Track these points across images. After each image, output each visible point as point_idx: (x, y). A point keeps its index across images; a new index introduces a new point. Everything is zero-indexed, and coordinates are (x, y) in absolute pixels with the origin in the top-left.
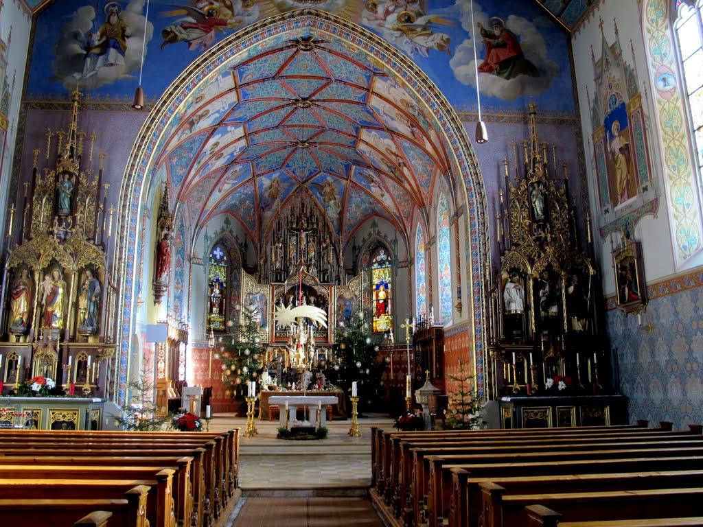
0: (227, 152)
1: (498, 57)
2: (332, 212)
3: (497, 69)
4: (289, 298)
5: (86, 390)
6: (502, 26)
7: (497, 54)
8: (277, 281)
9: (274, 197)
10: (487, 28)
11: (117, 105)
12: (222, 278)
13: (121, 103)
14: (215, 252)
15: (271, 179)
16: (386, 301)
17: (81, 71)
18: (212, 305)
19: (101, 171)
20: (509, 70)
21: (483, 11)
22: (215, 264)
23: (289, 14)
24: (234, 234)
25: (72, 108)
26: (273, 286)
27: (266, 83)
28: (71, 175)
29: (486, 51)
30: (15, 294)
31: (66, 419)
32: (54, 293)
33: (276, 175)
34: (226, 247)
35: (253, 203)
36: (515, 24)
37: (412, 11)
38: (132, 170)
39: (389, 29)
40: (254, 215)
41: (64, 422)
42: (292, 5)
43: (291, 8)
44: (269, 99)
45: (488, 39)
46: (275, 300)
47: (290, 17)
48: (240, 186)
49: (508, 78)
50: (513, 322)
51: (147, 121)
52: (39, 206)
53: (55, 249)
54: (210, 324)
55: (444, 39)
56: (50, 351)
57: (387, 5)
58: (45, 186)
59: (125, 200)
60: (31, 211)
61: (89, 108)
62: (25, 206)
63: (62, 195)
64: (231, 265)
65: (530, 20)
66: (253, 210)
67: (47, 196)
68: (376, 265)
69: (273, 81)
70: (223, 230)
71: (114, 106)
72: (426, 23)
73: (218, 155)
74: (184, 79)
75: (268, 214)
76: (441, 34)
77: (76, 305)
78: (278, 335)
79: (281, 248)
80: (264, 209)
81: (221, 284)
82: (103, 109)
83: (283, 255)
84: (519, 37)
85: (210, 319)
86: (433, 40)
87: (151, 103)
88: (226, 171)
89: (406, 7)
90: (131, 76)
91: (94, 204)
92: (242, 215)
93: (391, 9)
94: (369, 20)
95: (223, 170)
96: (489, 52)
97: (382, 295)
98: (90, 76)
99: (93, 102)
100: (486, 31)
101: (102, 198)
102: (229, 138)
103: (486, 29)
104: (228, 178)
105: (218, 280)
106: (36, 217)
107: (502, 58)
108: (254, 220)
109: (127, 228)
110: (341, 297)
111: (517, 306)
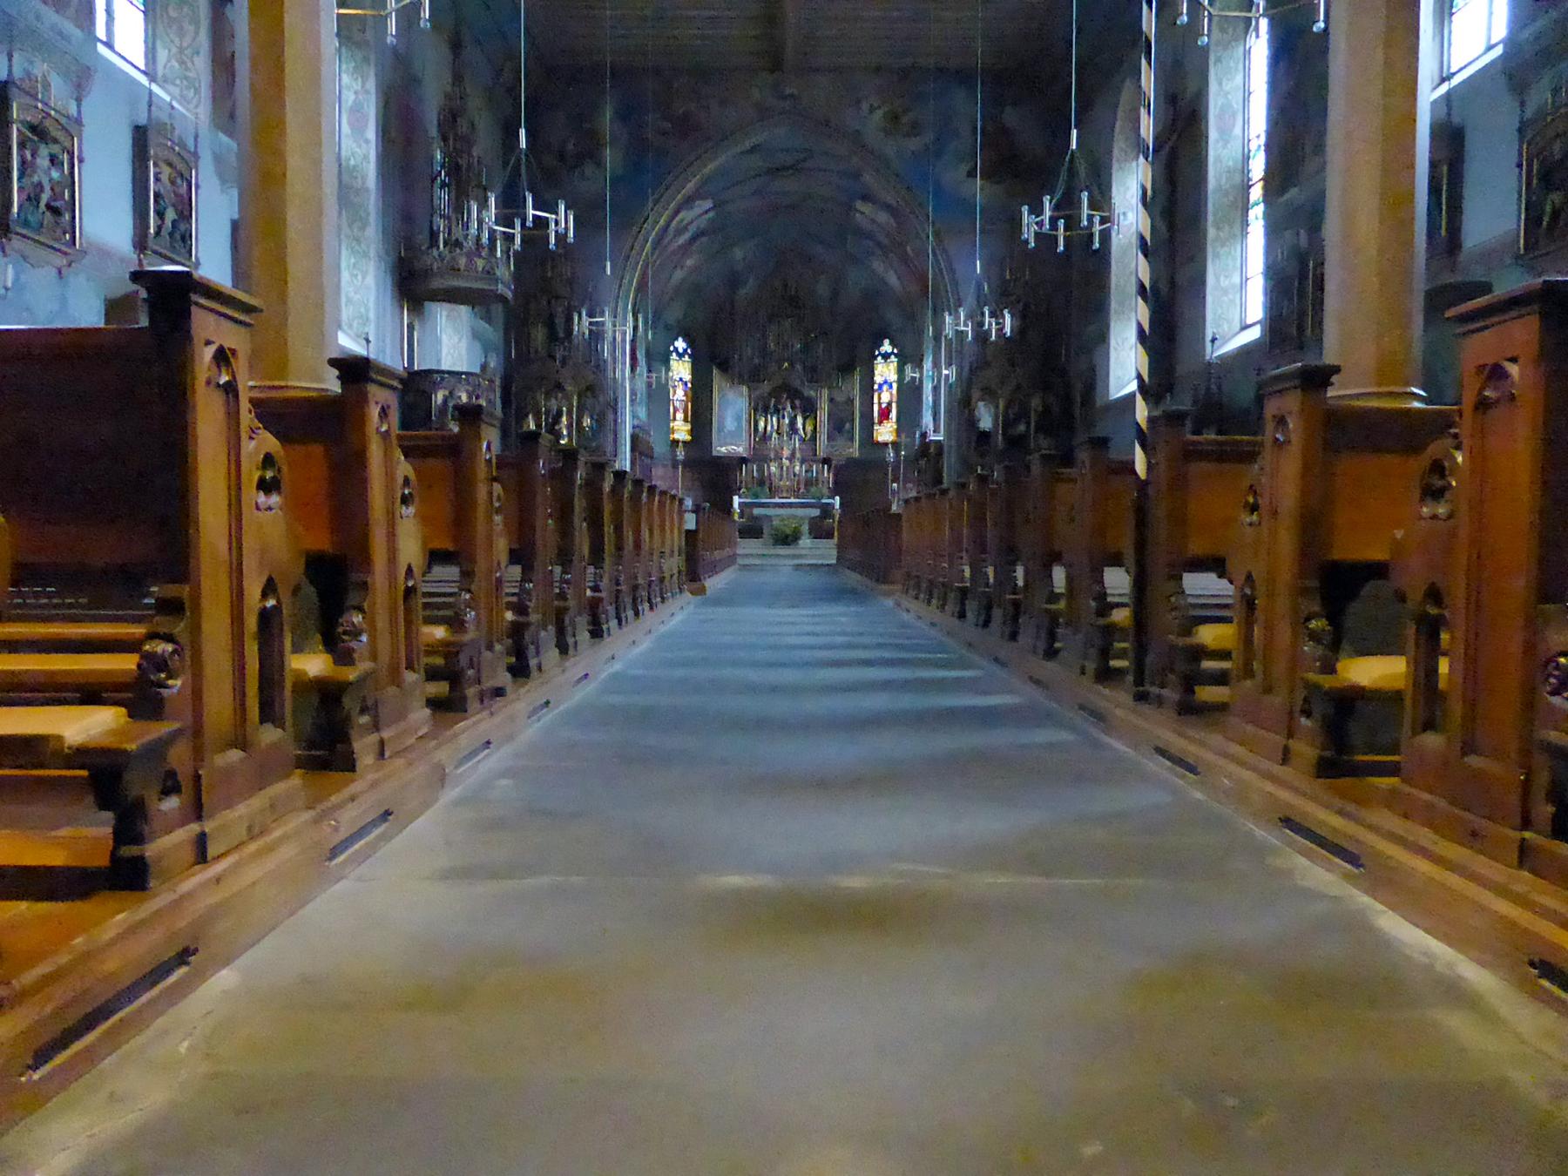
2: (823, 289)
14: (676, 344)
16: (889, 404)
18: (676, 410)
32: (559, 414)
36: (1011, 116)
50: (984, 436)
51: (630, 240)
68: (879, 358)
73: (679, 232)
75: (742, 292)
77: (579, 422)
81: (686, 384)
93: (876, 105)
97: (885, 397)
102: (697, 211)
105: (681, 379)
110: (831, 400)
111: (986, 422)
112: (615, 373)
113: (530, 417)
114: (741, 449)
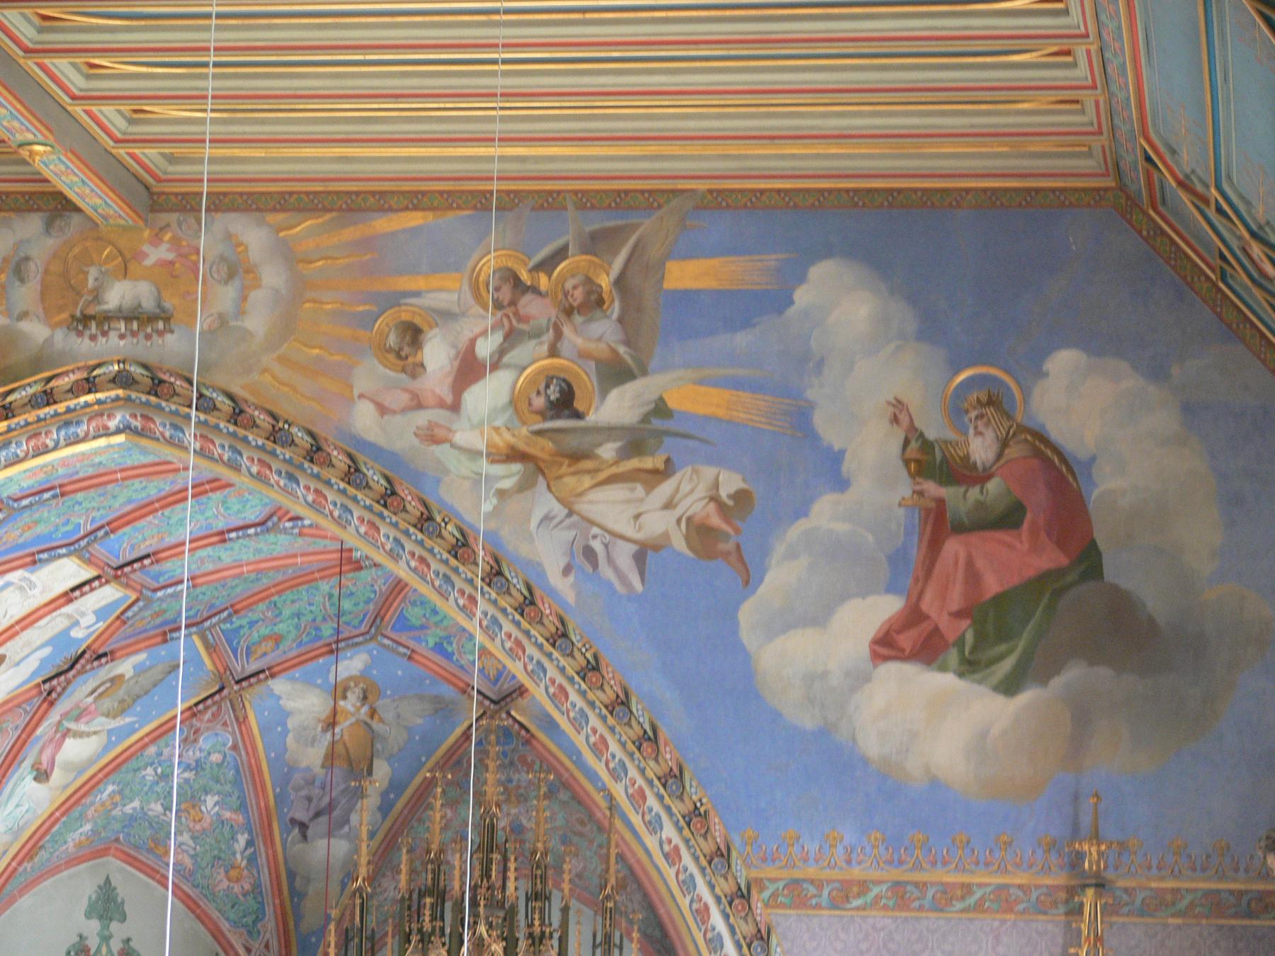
1: (973, 577)
3: (960, 642)
6: (1009, 417)
7: (970, 564)
10: (935, 428)
20: (1022, 644)
21: (921, 336)
23: (37, 388)
29: (915, 553)
33: (353, 664)
35: (242, 807)
37: (583, 355)
39: (474, 454)
40: (252, 860)
42: (49, 342)
43: (37, 363)
45: (931, 488)
47: (33, 403)
49: (1009, 687)
55: (724, 493)
57: (467, 329)
65: (1157, 372)
66: (242, 839)
72: (645, 419)
76: (709, 472)
80: (303, 827)
84: (1093, 459)
86: (669, 505)
89: (559, 335)
93: (485, 349)
94: (383, 410)
96: (935, 545)
100: (927, 446)
103: (931, 435)
104: (80, 714)
107: (992, 585)
108: (257, 888)
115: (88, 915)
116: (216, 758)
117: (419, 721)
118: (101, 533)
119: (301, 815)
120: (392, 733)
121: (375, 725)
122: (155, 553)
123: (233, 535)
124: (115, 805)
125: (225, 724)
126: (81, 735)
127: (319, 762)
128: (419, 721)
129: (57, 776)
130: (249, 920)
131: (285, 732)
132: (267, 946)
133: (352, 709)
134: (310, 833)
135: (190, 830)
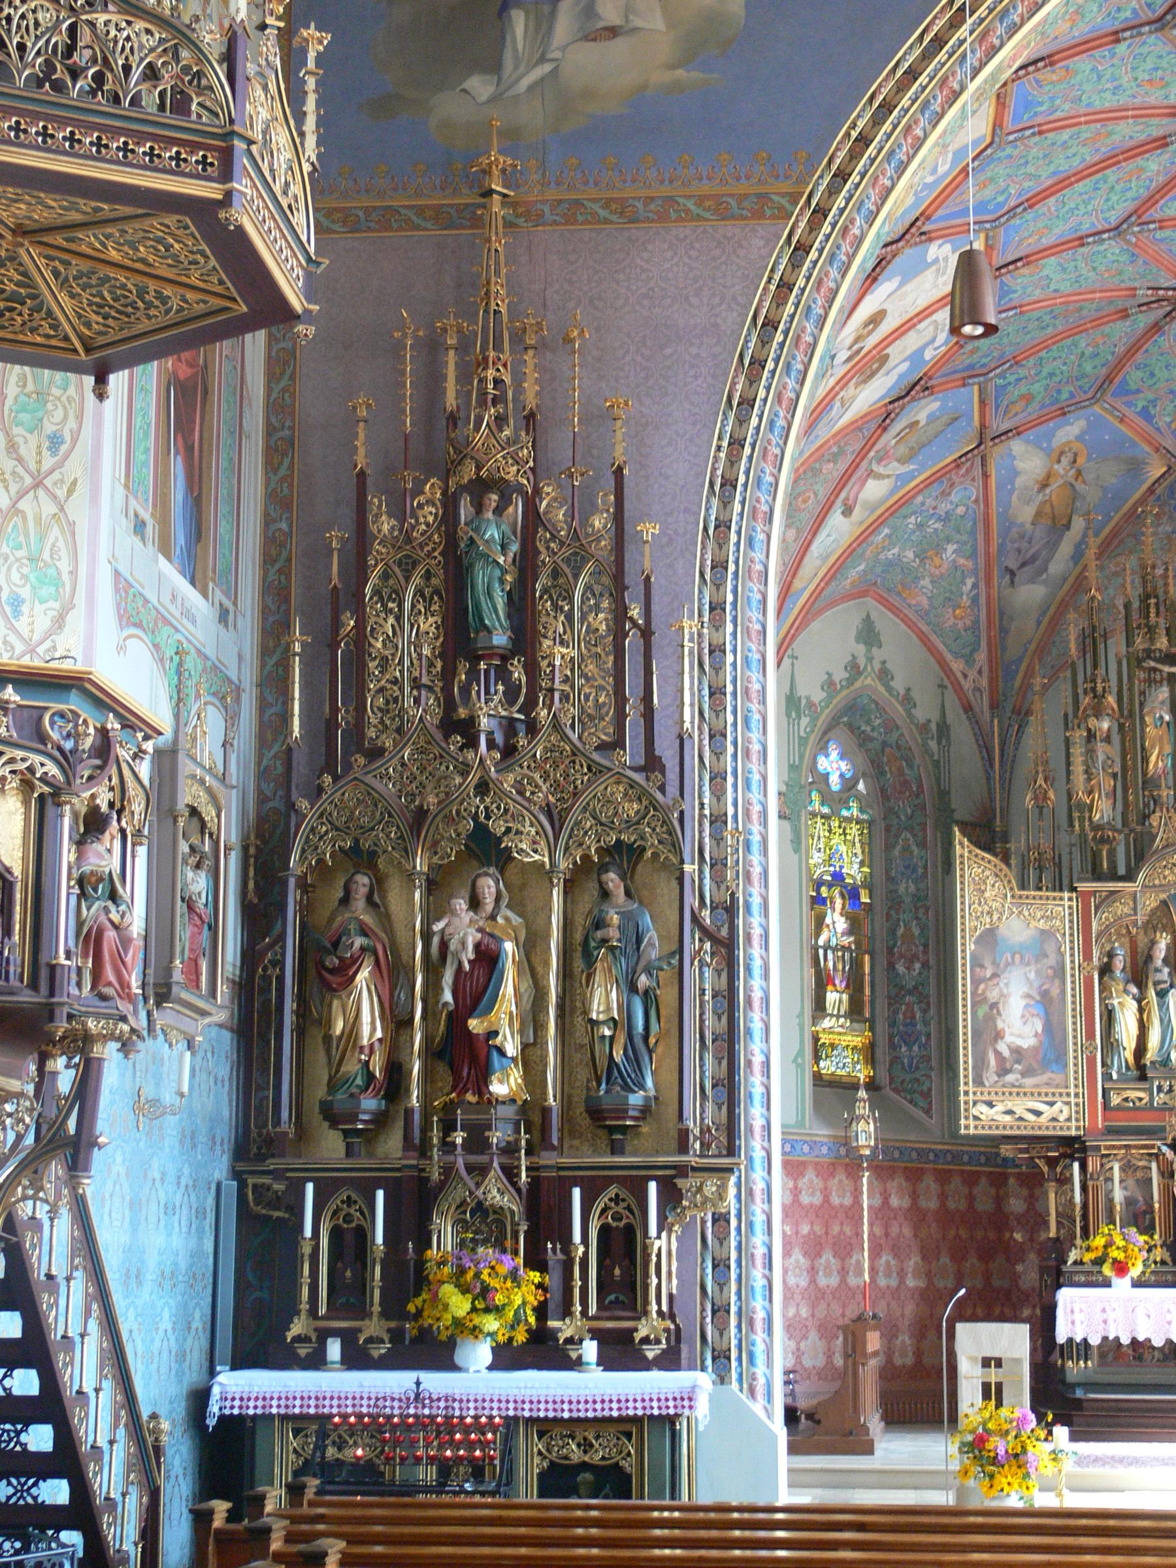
0: (898, 352)
4: (1153, 943)
5: (646, 1340)
8: (1098, 876)
9: (1058, 525)
11: (652, 199)
12: (854, 871)
13: (665, 190)
15: (1048, 452)
17: (493, 66)
18: (822, 981)
19: (619, 473)
22: (826, 810)
24: (899, 685)
25: (477, 222)
26: (1085, 897)
27: (1121, 48)
28: (506, 491)
30: (332, 971)
31: (596, 1457)
32: (488, 959)
33: (1069, 431)
34: (863, 740)
38: (733, 460)
40: (975, 600)
41: (584, 1466)
44: (1115, 115)
46: (1096, 953)
48: (928, 483)
52: (391, 620)
53: (483, 788)
54: (817, 1058)
56: (496, 1193)
58: (409, 540)
59: (718, 585)
60: (360, 639)
61: (541, 215)
62: (336, 624)
63: (481, 576)
64: (889, 813)
66: (969, 582)
67: (416, 580)
69: (1152, 39)
70: (854, 669)
71: (640, 205)
74: (912, 74)
78: (1115, 1100)
79: (1108, 739)
80: (1012, 574)
82: (595, 219)
83: (1117, 768)
85: (816, 1039)
87: (786, 187)
88: (883, 428)
90: (696, 75)
91: (605, 604)
92: (925, 602)
95: (873, 426)
98: (531, 88)
99: (552, 194)
101: (632, 578)
105: (838, 877)
106: (384, 663)
108: (976, 623)
109: (735, 694)
112: (719, 794)
113: (363, 975)
114: (1060, 1110)
115: (857, 641)
116: (961, 510)
117: (1114, 481)
118: (1019, 210)
119: (1013, 564)
120: (1090, 493)
121: (1079, 486)
122: (1027, 256)
123: (1091, 239)
124: (883, 548)
125: (973, 480)
126: (879, 477)
127: (1030, 519)
128: (1114, 481)
129: (857, 512)
130: (967, 650)
131: (1013, 489)
132: (980, 672)
133: (1062, 472)
134: (1017, 579)
135: (931, 575)
